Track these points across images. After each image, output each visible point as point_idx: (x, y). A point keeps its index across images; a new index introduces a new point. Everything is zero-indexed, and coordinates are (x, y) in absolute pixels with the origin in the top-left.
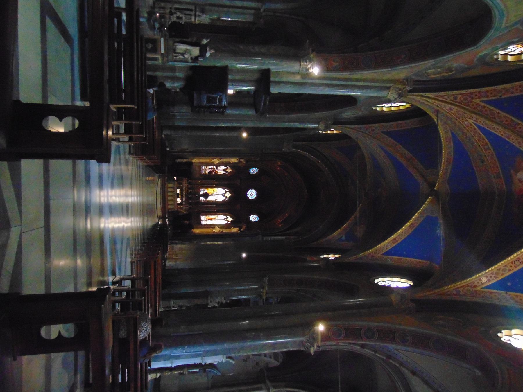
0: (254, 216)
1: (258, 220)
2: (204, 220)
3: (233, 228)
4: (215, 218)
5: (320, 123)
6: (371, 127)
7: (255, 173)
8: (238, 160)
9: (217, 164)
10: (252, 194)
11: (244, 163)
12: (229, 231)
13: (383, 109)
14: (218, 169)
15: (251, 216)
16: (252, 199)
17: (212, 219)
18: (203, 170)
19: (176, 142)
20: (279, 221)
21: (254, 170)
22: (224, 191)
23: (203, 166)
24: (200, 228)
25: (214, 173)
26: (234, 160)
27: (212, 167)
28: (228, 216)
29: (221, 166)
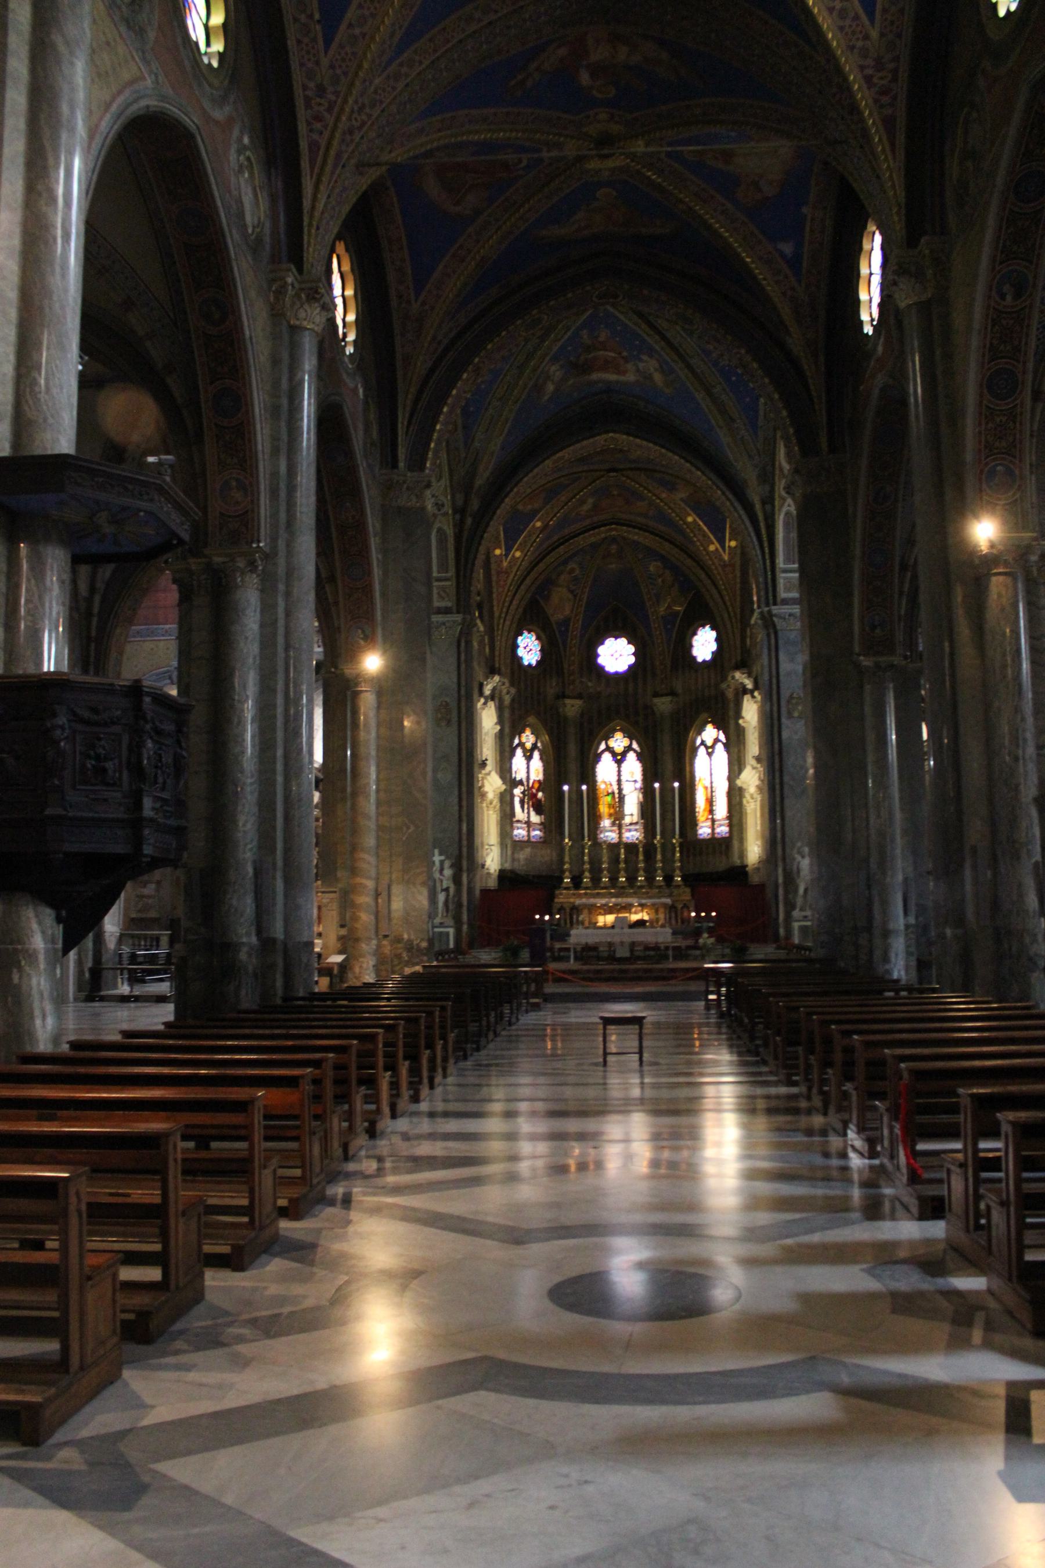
1: (713, 629)
4: (706, 788)
5: (297, 323)
6: (308, 100)
7: (536, 642)
8: (485, 704)
9: (504, 783)
10: (616, 655)
11: (497, 678)
12: (756, 735)
13: (216, 27)
14: (524, 780)
15: (694, 658)
16: (634, 654)
18: (529, 831)
19: (406, 936)
20: (717, 549)
22: (607, 757)
23: (516, 832)
24: (742, 840)
25: (540, 795)
26: (488, 719)
27: (517, 800)
28: (698, 742)
29: (514, 768)
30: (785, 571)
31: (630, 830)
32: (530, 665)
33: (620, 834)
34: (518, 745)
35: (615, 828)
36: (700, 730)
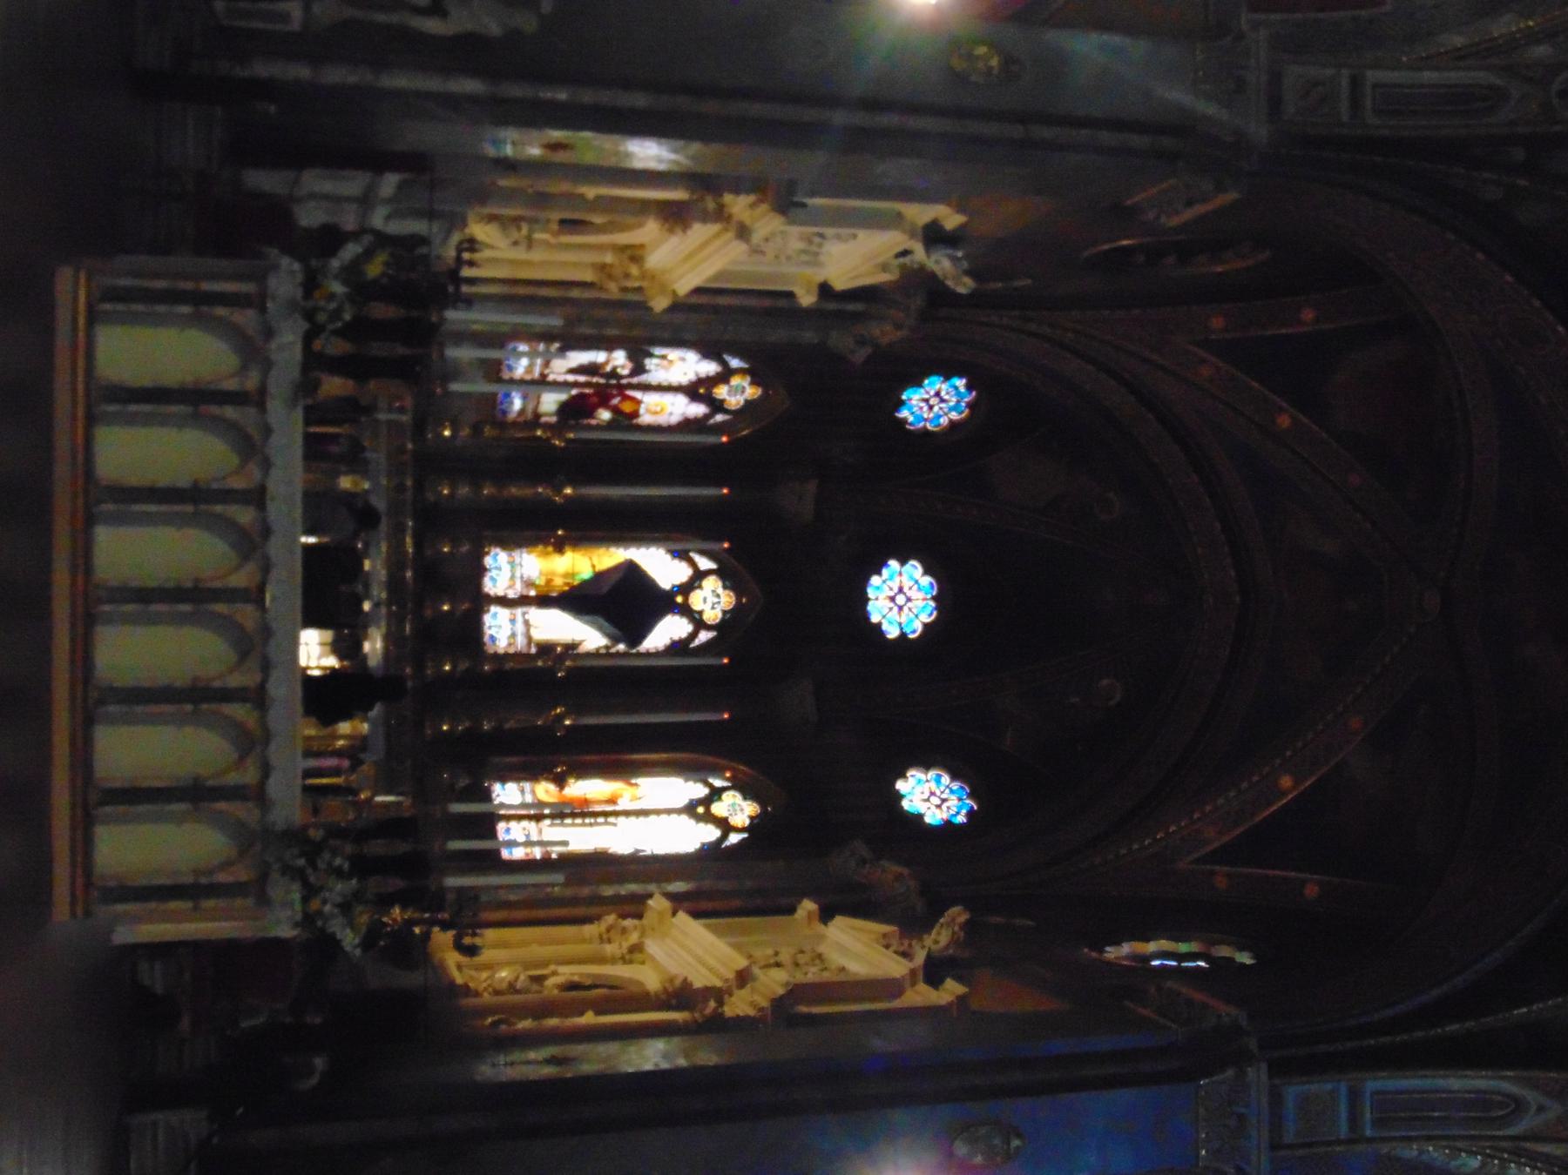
0: (932, 774)
1: (971, 814)
2: (520, 818)
3: (826, 915)
4: (612, 801)
7: (944, 421)
10: (901, 600)
14: (644, 378)
15: (903, 775)
16: (903, 635)
17: (586, 802)
21: (938, 394)
25: (605, 415)
27: (599, 357)
28: (718, 783)
29: (674, 354)
30: (1354, 1096)
31: (513, 621)
32: (902, 403)
33: (504, 601)
34: (724, 364)
35: (519, 587)
36: (748, 792)
